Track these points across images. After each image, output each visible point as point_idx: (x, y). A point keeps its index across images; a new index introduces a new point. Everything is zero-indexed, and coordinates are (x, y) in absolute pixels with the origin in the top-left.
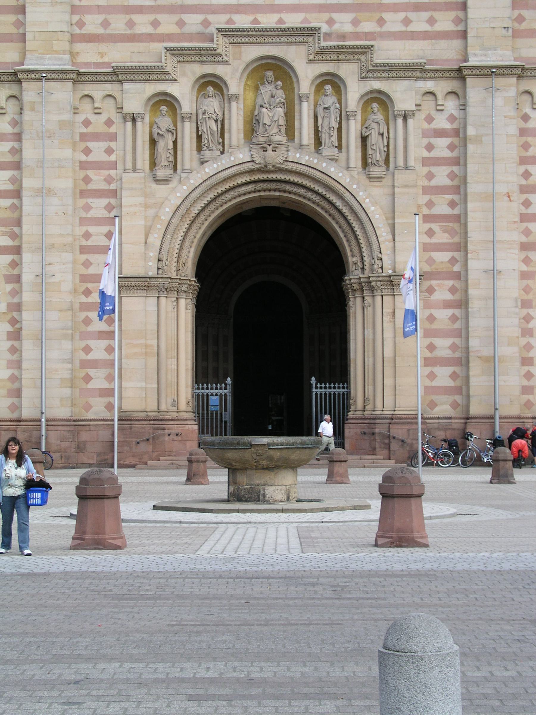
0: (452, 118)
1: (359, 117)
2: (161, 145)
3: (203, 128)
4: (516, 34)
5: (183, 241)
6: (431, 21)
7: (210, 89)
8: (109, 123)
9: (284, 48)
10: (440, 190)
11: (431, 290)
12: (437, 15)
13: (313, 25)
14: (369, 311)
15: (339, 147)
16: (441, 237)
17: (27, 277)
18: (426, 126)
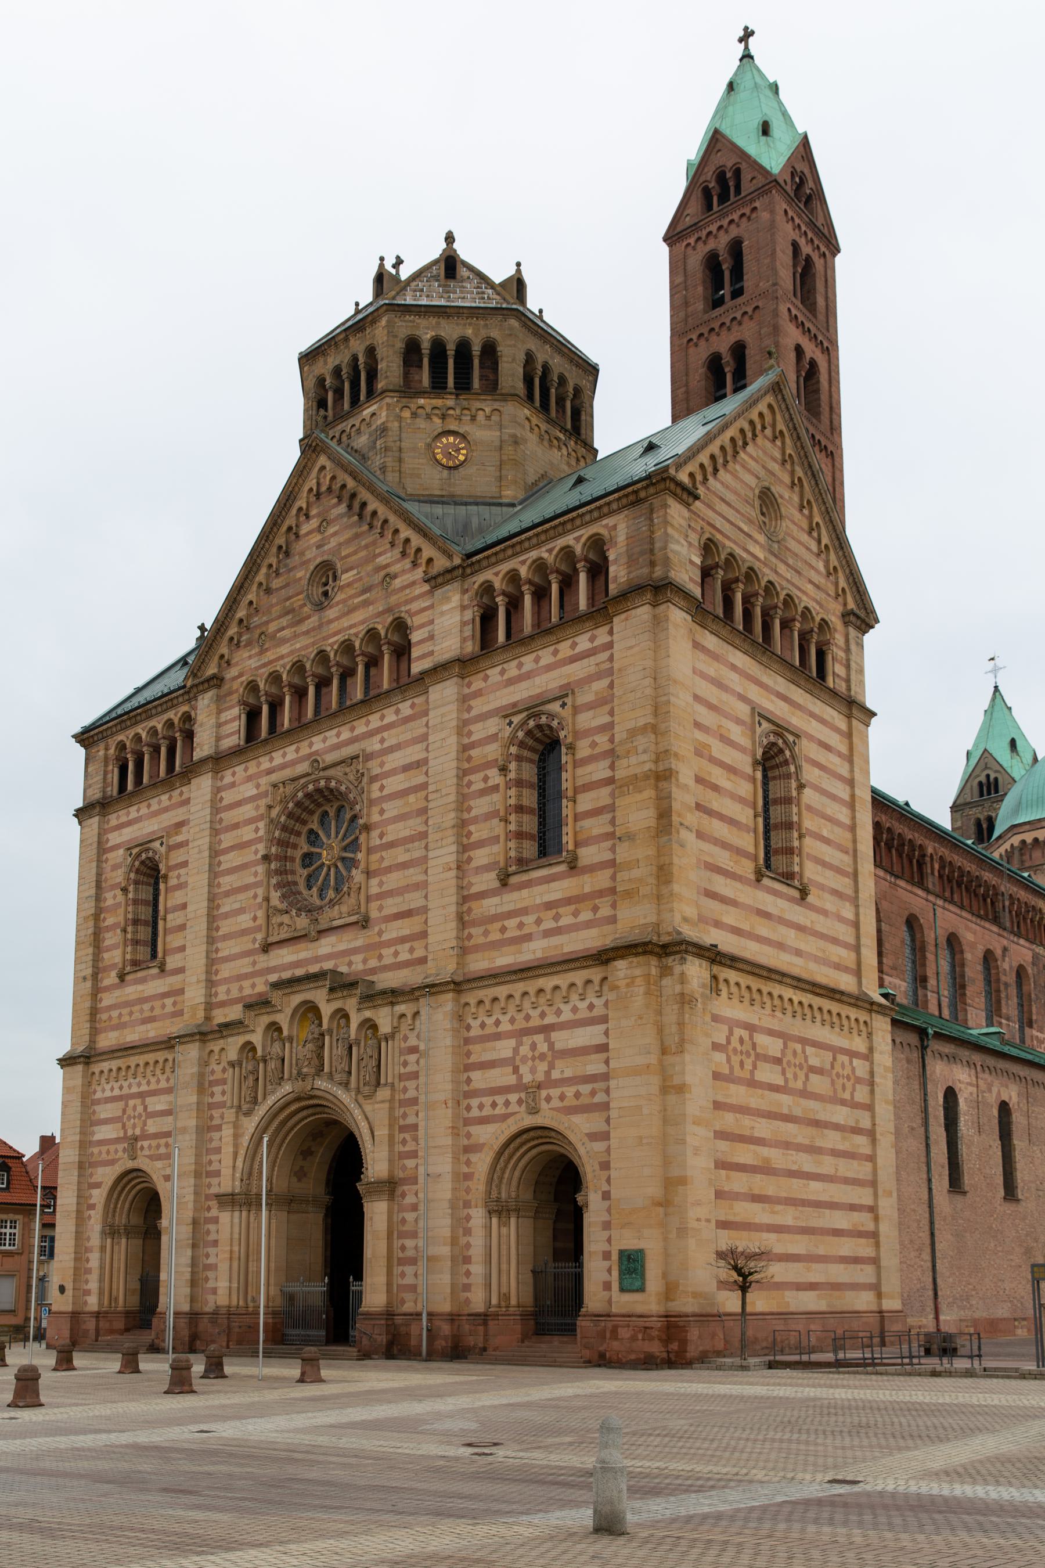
6: (412, 950)
8: (224, 1070)
9: (314, 992)
12: (416, 944)
15: (350, 1073)
18: (403, 1045)
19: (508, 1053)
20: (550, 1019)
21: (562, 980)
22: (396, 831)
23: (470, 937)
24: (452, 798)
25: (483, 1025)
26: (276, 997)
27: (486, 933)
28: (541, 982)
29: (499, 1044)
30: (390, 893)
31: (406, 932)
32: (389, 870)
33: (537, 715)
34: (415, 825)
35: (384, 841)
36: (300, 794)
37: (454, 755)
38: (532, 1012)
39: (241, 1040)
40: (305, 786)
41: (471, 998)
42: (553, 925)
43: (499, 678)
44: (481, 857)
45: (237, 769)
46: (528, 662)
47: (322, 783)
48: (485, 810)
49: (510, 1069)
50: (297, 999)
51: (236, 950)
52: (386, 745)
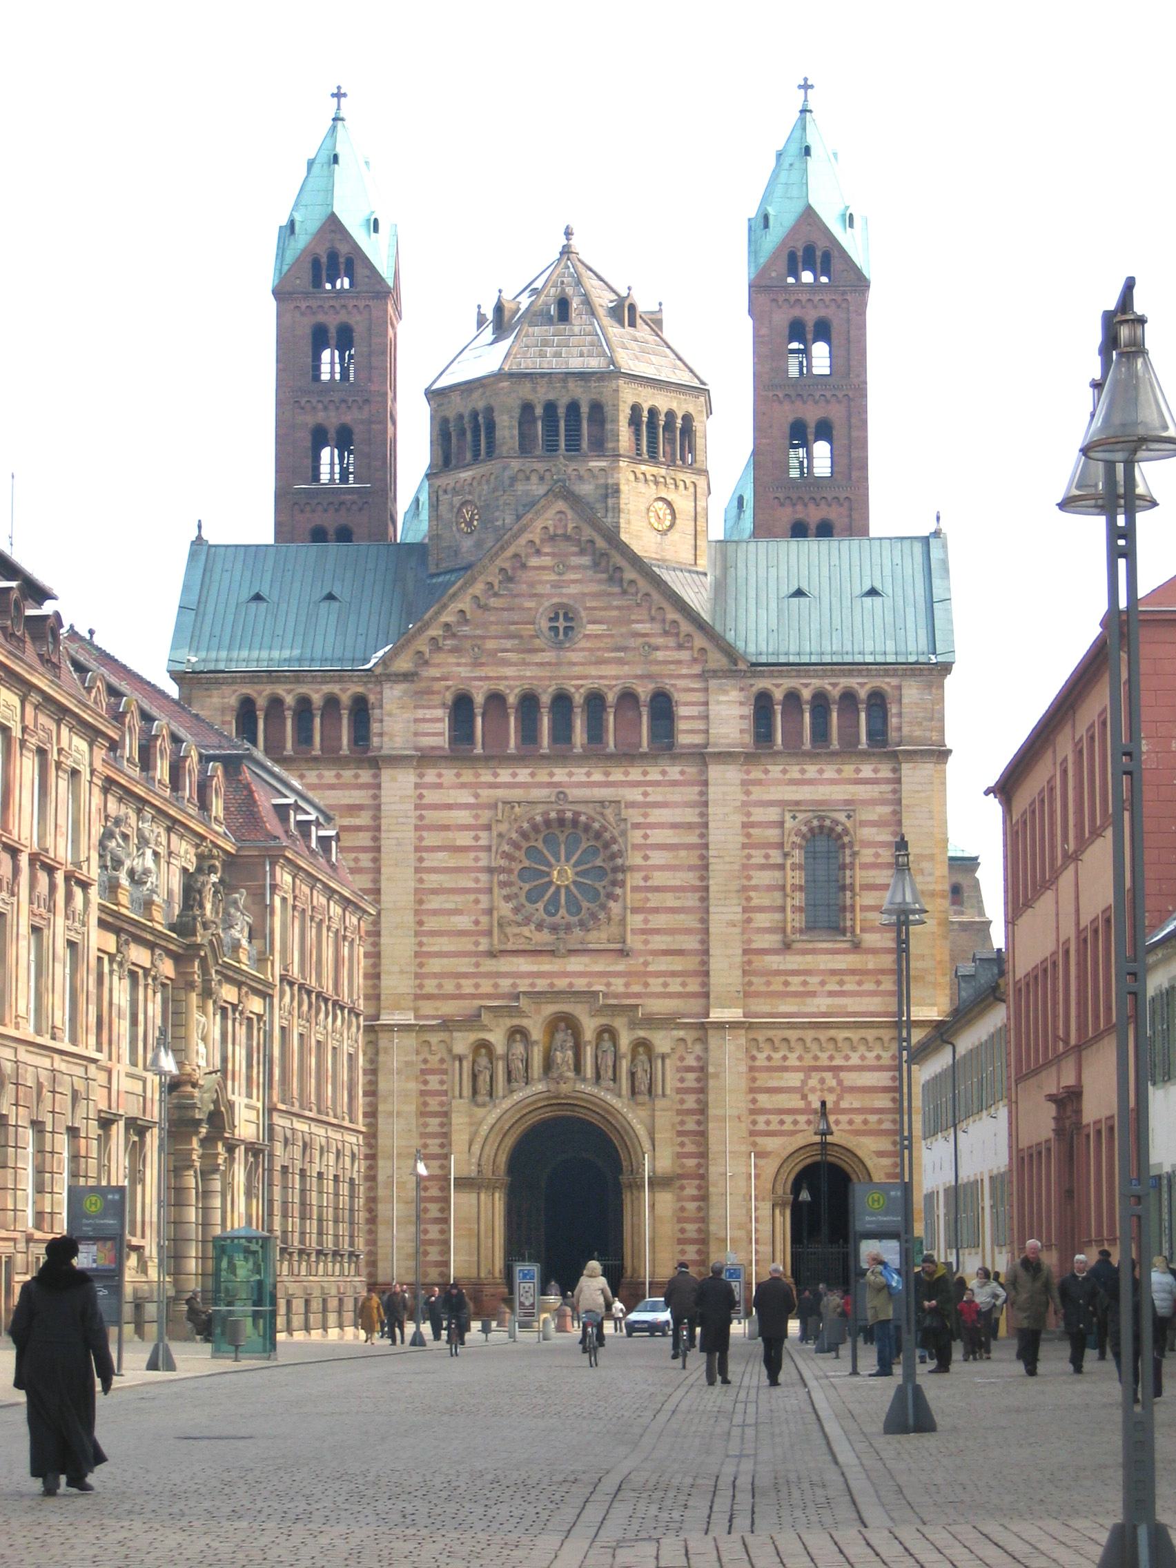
0: (699, 1058)
1: (629, 1057)
2: (481, 1078)
3: (512, 1066)
4: (747, 995)
5: (497, 1150)
6: (684, 984)
7: (518, 1037)
8: (442, 1061)
10: (690, 1112)
11: (682, 1188)
12: (689, 980)
13: (593, 989)
14: (636, 1203)
15: (614, 1080)
16: (690, 1148)
17: (381, 1177)
18: (679, 1064)
19: (798, 1084)
20: (838, 1062)
21: (854, 1035)
22: (659, 879)
23: (750, 984)
24: (737, 867)
25: (769, 1058)
26: (523, 1003)
27: (768, 983)
28: (832, 1033)
29: (785, 1074)
30: (657, 931)
31: (679, 968)
32: (656, 910)
33: (822, 818)
34: (691, 878)
35: (648, 884)
36: (538, 818)
37: (739, 831)
38: (819, 1054)
39: (473, 1037)
40: (545, 813)
41: (761, 1036)
42: (837, 988)
43: (780, 776)
44: (762, 920)
45: (444, 771)
46: (812, 771)
47: (569, 815)
48: (767, 882)
49: (799, 1096)
50: (550, 1009)
51: (452, 948)
52: (649, 799)
